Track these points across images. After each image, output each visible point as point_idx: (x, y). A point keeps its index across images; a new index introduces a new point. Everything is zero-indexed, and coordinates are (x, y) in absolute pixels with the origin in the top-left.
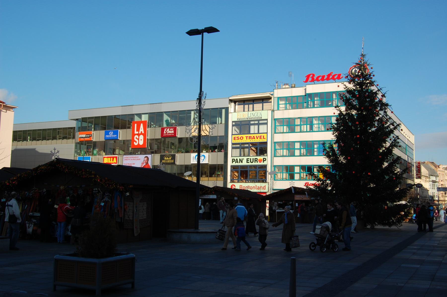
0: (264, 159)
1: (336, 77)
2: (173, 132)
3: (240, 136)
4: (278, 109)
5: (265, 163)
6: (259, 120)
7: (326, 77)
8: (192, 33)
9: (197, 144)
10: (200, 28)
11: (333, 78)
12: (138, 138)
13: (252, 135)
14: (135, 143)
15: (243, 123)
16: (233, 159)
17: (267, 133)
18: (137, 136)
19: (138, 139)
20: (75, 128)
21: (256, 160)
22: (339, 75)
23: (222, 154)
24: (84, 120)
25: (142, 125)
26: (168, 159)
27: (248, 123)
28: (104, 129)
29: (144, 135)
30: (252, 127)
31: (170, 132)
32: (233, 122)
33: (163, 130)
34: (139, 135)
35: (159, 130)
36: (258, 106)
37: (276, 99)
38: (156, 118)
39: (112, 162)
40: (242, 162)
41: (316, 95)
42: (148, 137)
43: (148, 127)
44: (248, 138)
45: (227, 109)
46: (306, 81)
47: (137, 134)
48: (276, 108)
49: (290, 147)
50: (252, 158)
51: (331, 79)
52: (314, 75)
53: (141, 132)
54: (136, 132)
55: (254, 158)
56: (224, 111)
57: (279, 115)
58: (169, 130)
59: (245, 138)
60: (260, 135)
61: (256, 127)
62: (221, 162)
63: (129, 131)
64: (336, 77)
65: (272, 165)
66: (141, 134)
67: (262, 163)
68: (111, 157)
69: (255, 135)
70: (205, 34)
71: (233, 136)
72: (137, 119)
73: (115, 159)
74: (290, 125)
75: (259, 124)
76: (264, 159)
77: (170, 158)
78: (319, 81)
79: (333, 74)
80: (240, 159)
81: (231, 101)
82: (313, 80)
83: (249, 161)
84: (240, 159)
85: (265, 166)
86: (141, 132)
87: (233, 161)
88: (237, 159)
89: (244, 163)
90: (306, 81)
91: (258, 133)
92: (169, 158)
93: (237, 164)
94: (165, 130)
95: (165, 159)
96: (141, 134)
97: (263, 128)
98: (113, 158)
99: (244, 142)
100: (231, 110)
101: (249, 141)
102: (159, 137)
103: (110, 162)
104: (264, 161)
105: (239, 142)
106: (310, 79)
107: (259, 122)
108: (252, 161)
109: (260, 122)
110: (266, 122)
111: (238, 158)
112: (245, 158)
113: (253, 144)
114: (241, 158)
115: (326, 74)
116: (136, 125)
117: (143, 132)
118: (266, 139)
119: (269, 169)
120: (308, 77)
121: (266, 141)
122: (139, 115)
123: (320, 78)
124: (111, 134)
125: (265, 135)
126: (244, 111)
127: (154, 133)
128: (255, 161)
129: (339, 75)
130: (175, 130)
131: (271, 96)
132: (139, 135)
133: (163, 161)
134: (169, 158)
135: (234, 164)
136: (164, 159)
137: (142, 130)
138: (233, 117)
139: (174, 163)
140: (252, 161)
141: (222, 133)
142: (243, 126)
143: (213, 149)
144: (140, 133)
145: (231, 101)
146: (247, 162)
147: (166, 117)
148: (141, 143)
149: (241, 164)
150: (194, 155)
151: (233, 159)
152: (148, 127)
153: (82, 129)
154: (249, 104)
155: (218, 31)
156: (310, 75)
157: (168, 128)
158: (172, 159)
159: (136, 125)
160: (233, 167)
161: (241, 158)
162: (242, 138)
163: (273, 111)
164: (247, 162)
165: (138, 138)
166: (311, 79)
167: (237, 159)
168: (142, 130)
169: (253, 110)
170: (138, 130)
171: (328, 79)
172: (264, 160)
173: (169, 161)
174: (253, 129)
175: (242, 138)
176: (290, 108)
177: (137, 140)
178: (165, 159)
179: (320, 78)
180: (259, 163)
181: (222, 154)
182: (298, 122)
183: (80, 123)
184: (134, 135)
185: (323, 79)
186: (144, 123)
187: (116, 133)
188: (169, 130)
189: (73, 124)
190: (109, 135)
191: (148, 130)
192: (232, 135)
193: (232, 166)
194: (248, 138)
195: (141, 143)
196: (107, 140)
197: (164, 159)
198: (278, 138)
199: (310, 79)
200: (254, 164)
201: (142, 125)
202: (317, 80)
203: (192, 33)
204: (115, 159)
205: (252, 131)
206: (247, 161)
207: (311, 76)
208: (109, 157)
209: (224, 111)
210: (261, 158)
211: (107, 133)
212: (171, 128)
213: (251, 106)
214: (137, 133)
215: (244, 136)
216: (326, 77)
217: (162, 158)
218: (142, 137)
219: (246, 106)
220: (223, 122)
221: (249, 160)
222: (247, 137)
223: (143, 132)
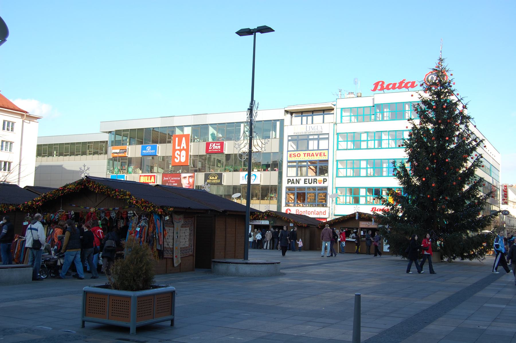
0: (324, 179)
1: (409, 85)
3: (297, 153)
4: (341, 122)
5: (326, 184)
6: (318, 135)
7: (397, 85)
8: (243, 33)
9: (247, 162)
10: (252, 28)
11: (406, 87)
13: (311, 152)
14: (176, 159)
15: (300, 137)
16: (288, 180)
17: (328, 150)
19: (180, 155)
20: (107, 141)
21: (315, 181)
22: (413, 83)
23: (276, 173)
24: (118, 132)
25: (184, 138)
26: (213, 178)
27: (306, 137)
28: (141, 143)
30: (311, 142)
31: (216, 147)
32: (289, 136)
33: (208, 144)
35: (203, 145)
36: (318, 118)
37: (339, 111)
38: (200, 130)
39: (149, 181)
40: (299, 183)
41: (386, 105)
42: (191, 153)
43: (191, 142)
44: (306, 155)
45: (282, 121)
46: (374, 90)
47: (178, 150)
48: (339, 121)
49: (355, 166)
50: (310, 178)
51: (403, 87)
52: (383, 83)
53: (183, 147)
54: (177, 147)
55: (313, 178)
56: (278, 123)
57: (342, 128)
58: (216, 145)
59: (302, 155)
60: (319, 152)
61: (316, 142)
62: (275, 182)
63: (170, 146)
64: (409, 85)
65: (334, 187)
66: (183, 149)
67: (322, 185)
68: (148, 176)
69: (314, 152)
70: (258, 34)
71: (289, 153)
72: (178, 132)
73: (153, 177)
74: (355, 140)
75: (318, 139)
76: (324, 179)
77: (216, 178)
78: (390, 89)
79: (406, 82)
80: (296, 180)
81: (287, 112)
82: (382, 89)
83: (307, 182)
84: (296, 180)
85: (326, 188)
86: (183, 147)
87: (288, 182)
88: (293, 180)
89: (302, 184)
90: (374, 90)
91: (318, 149)
92: (215, 177)
93: (293, 185)
94: (211, 145)
95: (211, 178)
96: (183, 149)
97: (323, 144)
98: (151, 176)
99: (302, 160)
100: (287, 122)
101: (307, 158)
102: (204, 153)
103: (147, 181)
104: (324, 182)
105: (295, 160)
106: (379, 87)
107: (318, 137)
108: (310, 182)
109: (319, 137)
110: (327, 136)
111: (295, 179)
112: (303, 179)
113: (312, 162)
114: (298, 178)
115: (397, 81)
116: (177, 139)
117: (185, 148)
118: (327, 157)
119: (330, 192)
120: (376, 84)
121: (327, 159)
122: (181, 128)
123: (390, 86)
124: (149, 150)
125: (326, 152)
126: (302, 124)
127: (198, 148)
128: (314, 181)
129: (413, 83)
130: (222, 144)
131: (333, 106)
132: (180, 150)
133: (208, 181)
134: (215, 177)
135: (290, 185)
136: (209, 179)
137: (184, 144)
138: (288, 131)
139: (220, 184)
140: (310, 182)
141: (276, 149)
142: (301, 141)
143: (266, 167)
144: (182, 148)
145: (287, 112)
146: (305, 183)
147: (211, 130)
148: (183, 160)
149: (297, 185)
150: (243, 174)
151: (288, 180)
152: (191, 142)
153: (116, 143)
154: (307, 116)
155: (273, 31)
156: (379, 82)
157: (213, 143)
158: (218, 179)
159: (177, 139)
160: (289, 189)
161: (298, 178)
162: (299, 155)
163: (336, 124)
164: (305, 183)
165: (179, 154)
166: (380, 86)
167: (293, 180)
168: (184, 144)
169: (312, 123)
170: (179, 145)
171: (400, 87)
172: (325, 181)
173: (214, 181)
174: (313, 145)
175: (299, 155)
176: (356, 121)
177: (178, 157)
178: (211, 178)
179: (390, 86)
180: (318, 185)
181: (276, 173)
182: (364, 137)
183: (113, 136)
184: (174, 150)
185: (394, 88)
186: (187, 136)
187: (154, 148)
188: (216, 145)
189: (106, 137)
190: (146, 150)
191: (192, 144)
192: (288, 151)
193: (287, 188)
194: (306, 155)
195: (183, 160)
196: (144, 156)
197: (209, 179)
198: (342, 155)
199: (379, 87)
200: (312, 185)
201: (184, 138)
202: (388, 88)
203: (243, 33)
204: (153, 177)
205: (310, 148)
206: (305, 181)
207: (380, 83)
208: (146, 176)
209: (278, 123)
210: (320, 178)
211: (143, 149)
212: (217, 143)
213: (310, 118)
214: (179, 148)
215: (302, 153)
216: (397, 85)
217: (207, 177)
218: (183, 153)
219: (304, 118)
220: (278, 136)
221: (307, 180)
222: (305, 154)
223: (185, 148)
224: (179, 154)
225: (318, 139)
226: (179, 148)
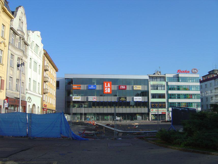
1: (188, 72)
2: (125, 87)
6: (161, 85)
12: (107, 89)
14: (105, 91)
18: (107, 89)
19: (107, 90)
22: (189, 71)
26: (123, 99)
29: (111, 88)
34: (108, 88)
47: (106, 88)
52: (180, 70)
53: (109, 87)
54: (106, 87)
61: (155, 87)
62: (146, 100)
66: (109, 87)
79: (187, 71)
82: (180, 72)
86: (109, 87)
96: (109, 87)
116: (106, 83)
117: (110, 87)
120: (178, 71)
127: (115, 87)
129: (189, 71)
132: (108, 88)
133: (121, 100)
137: (109, 85)
138: (151, 83)
144: (108, 87)
148: (109, 91)
156: (179, 70)
158: (125, 99)
159: (106, 83)
170: (107, 85)
177: (107, 90)
181: (146, 98)
185: (183, 72)
191: (112, 86)
195: (109, 91)
202: (182, 72)
214: (107, 87)
218: (109, 89)
223: (110, 87)
224: (107, 89)
225: (161, 87)
226: (107, 87)
